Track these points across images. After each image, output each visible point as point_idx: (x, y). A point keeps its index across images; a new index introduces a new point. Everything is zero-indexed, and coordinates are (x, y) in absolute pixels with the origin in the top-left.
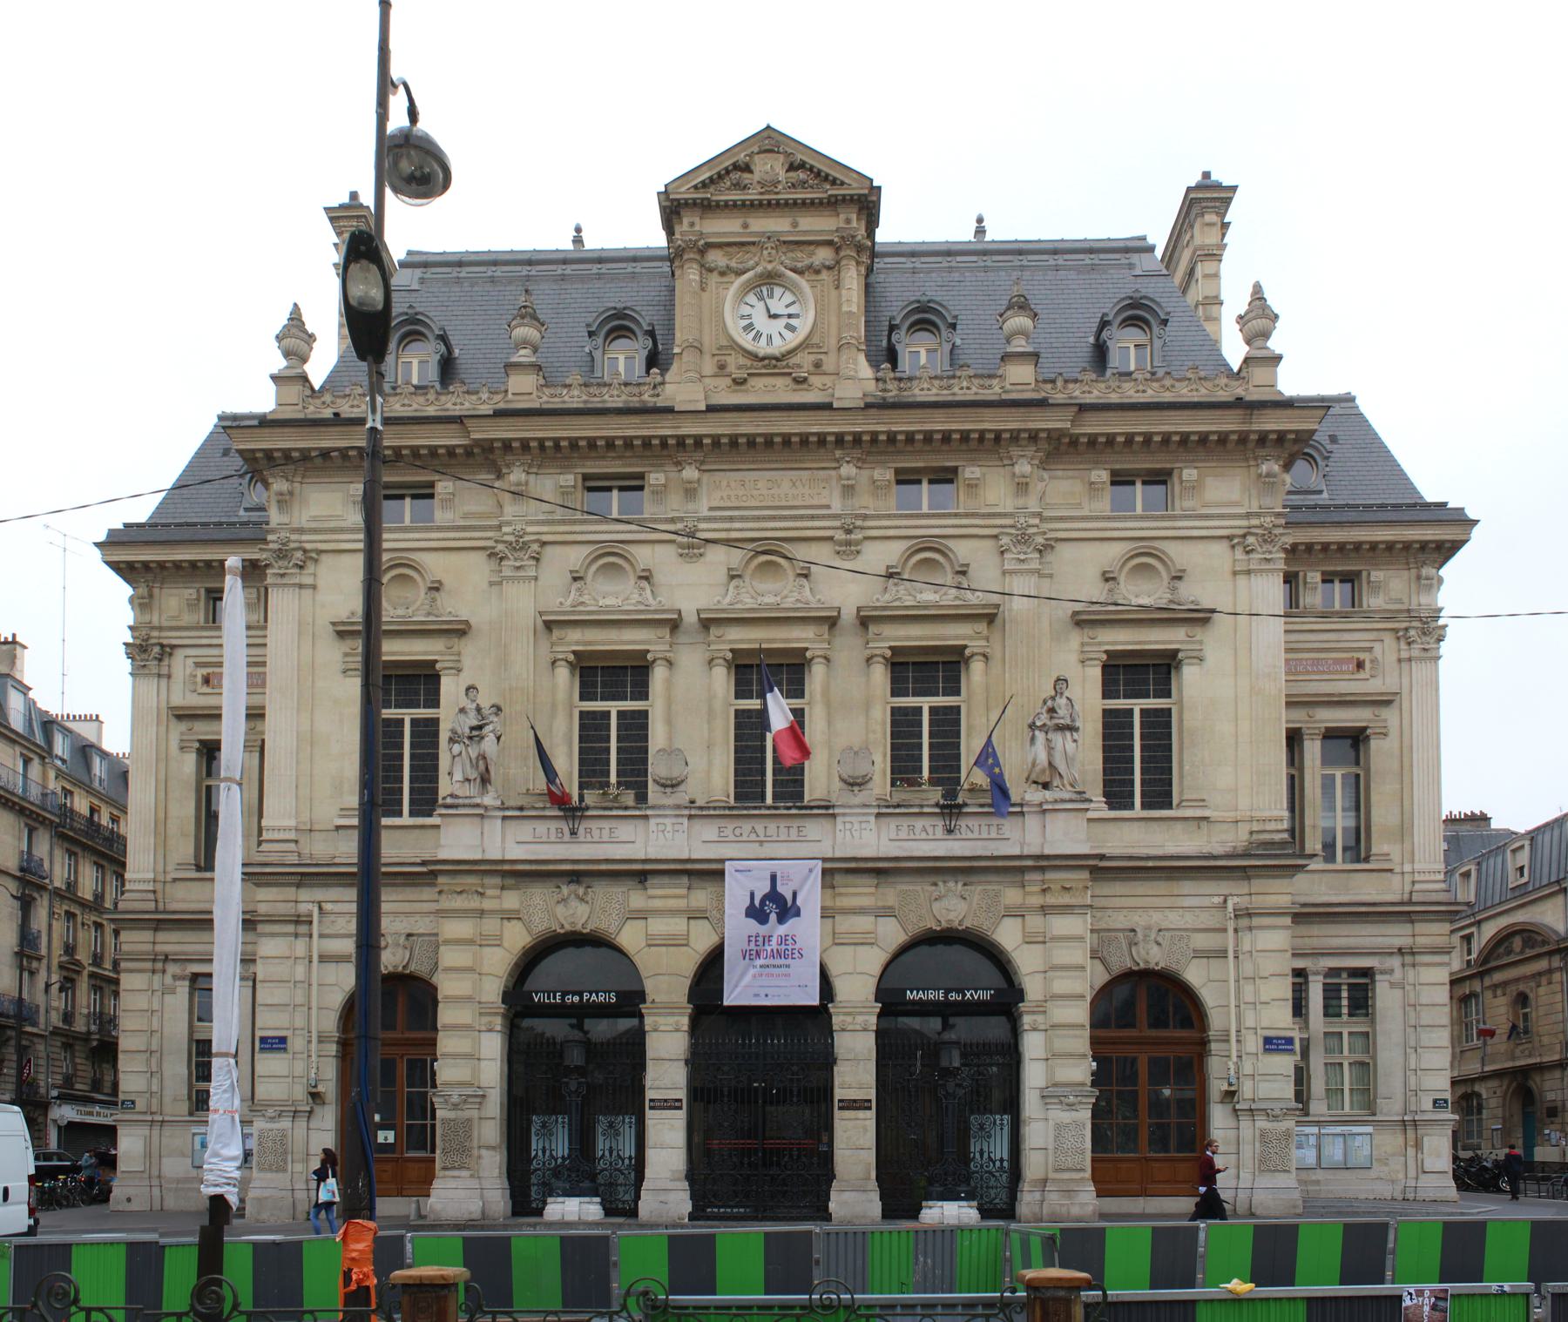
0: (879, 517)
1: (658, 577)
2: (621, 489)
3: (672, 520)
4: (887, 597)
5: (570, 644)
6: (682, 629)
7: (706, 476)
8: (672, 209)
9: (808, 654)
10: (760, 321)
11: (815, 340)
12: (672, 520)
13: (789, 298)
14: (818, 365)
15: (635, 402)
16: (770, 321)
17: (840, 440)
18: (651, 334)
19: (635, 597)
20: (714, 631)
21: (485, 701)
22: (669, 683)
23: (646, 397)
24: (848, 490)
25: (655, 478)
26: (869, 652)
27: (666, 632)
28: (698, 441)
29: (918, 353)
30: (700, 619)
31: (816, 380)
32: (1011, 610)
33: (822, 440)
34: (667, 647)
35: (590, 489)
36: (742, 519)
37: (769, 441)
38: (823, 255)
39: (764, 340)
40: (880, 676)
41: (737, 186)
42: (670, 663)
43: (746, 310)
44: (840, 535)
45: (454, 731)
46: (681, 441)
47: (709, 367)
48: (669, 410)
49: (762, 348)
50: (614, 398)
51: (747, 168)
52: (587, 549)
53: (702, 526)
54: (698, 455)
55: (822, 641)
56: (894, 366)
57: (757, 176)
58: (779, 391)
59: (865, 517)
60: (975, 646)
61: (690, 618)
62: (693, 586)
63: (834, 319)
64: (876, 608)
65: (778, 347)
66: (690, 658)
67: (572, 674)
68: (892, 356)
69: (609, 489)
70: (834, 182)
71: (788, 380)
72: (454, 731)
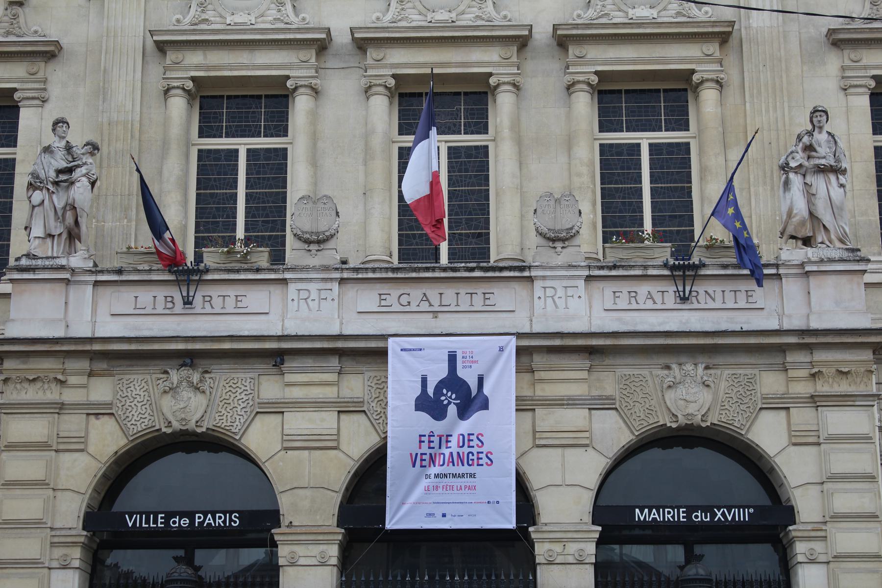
4: (591, 13)
5: (188, 69)
6: (331, 50)
9: (492, 81)
20: (373, 54)
21: (77, 137)
22: (314, 117)
26: (569, 78)
27: (310, 55)
30: (354, 39)
32: (748, 28)
34: (312, 73)
42: (316, 92)
45: (35, 175)
55: (512, 65)
60: (704, 70)
61: (342, 38)
64: (576, 26)
66: (342, 84)
67: (190, 104)
72: (35, 175)
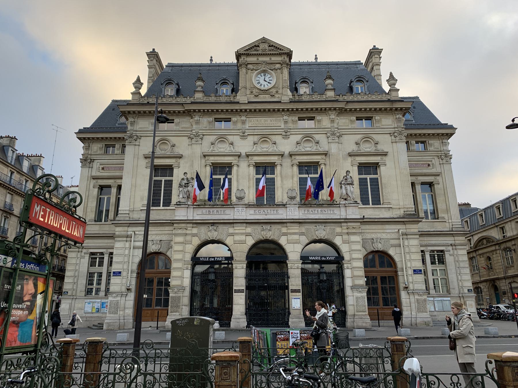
0: (294, 129)
1: (235, 144)
2: (225, 121)
3: (239, 130)
5: (210, 160)
7: (247, 119)
8: (238, 55)
10: (262, 82)
11: (276, 86)
12: (239, 130)
13: (269, 76)
14: (277, 92)
15: (228, 101)
16: (264, 81)
17: (283, 110)
18: (233, 84)
19: (229, 149)
22: (237, 171)
23: (231, 99)
24: (286, 122)
25: (234, 119)
28: (246, 110)
29: (304, 89)
31: (277, 96)
33: (279, 110)
35: (216, 121)
36: (257, 129)
37: (264, 110)
38: (278, 66)
39: (263, 86)
40: (296, 169)
41: (255, 50)
43: (258, 79)
44: (284, 134)
46: (241, 110)
47: (248, 92)
48: (238, 103)
49: (262, 88)
50: (223, 99)
51: (258, 46)
52: (216, 136)
53: (246, 131)
54: (246, 114)
56: (297, 92)
57: (261, 48)
58: (267, 98)
59: (290, 129)
61: (243, 154)
62: (244, 146)
63: (281, 81)
65: (266, 87)
68: (296, 90)
69: (221, 121)
70: (281, 49)
71: (269, 95)
